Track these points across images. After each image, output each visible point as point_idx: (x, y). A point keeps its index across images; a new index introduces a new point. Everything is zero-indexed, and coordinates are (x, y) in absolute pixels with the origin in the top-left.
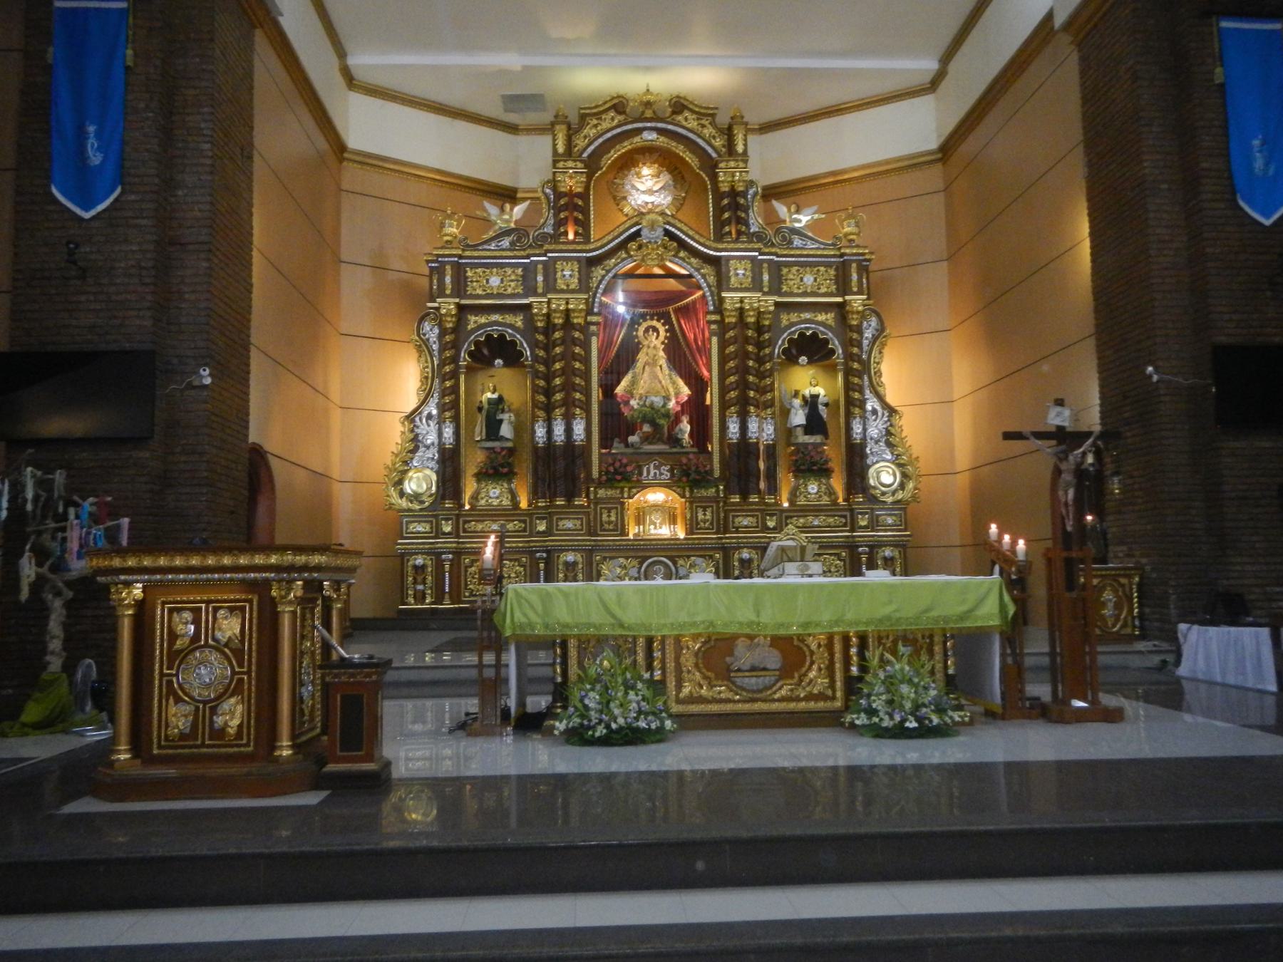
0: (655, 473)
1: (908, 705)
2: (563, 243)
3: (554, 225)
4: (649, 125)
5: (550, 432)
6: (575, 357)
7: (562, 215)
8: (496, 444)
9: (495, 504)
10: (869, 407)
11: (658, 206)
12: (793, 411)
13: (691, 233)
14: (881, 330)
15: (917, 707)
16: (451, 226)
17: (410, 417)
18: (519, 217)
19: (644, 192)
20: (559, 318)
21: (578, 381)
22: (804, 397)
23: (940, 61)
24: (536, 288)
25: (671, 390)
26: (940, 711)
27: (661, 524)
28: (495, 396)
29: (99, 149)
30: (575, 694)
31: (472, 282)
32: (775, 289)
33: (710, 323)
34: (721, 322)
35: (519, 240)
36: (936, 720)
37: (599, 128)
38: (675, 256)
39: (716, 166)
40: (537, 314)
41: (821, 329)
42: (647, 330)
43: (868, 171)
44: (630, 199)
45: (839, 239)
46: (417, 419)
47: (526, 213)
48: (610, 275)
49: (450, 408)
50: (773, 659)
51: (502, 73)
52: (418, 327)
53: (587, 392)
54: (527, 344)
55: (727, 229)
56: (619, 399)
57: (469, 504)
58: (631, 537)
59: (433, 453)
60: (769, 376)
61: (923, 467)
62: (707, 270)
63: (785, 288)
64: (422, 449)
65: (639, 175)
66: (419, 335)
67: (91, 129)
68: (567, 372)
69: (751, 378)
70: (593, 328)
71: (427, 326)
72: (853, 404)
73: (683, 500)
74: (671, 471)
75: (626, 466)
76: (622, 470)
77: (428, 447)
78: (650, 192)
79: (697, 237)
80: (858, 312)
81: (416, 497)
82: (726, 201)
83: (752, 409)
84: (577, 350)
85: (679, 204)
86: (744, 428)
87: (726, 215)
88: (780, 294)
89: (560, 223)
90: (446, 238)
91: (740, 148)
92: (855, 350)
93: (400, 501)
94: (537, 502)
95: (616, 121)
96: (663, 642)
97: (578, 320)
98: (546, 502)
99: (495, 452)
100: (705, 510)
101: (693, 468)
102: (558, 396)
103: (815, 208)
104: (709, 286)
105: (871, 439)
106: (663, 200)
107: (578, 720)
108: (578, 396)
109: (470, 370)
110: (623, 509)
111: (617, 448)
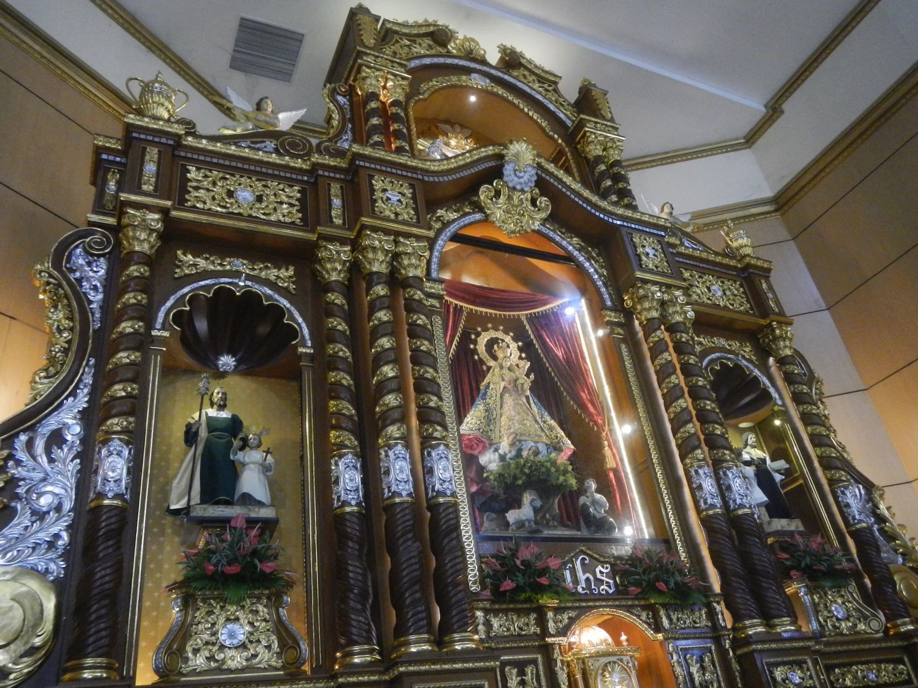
0: (588, 580)
9: (232, 664)
23: (766, 106)
28: (225, 415)
31: (197, 188)
42: (491, 343)
54: (302, 315)
59: (59, 527)
73: (660, 636)
86: (724, 490)
98: (371, 652)
110: (550, 664)
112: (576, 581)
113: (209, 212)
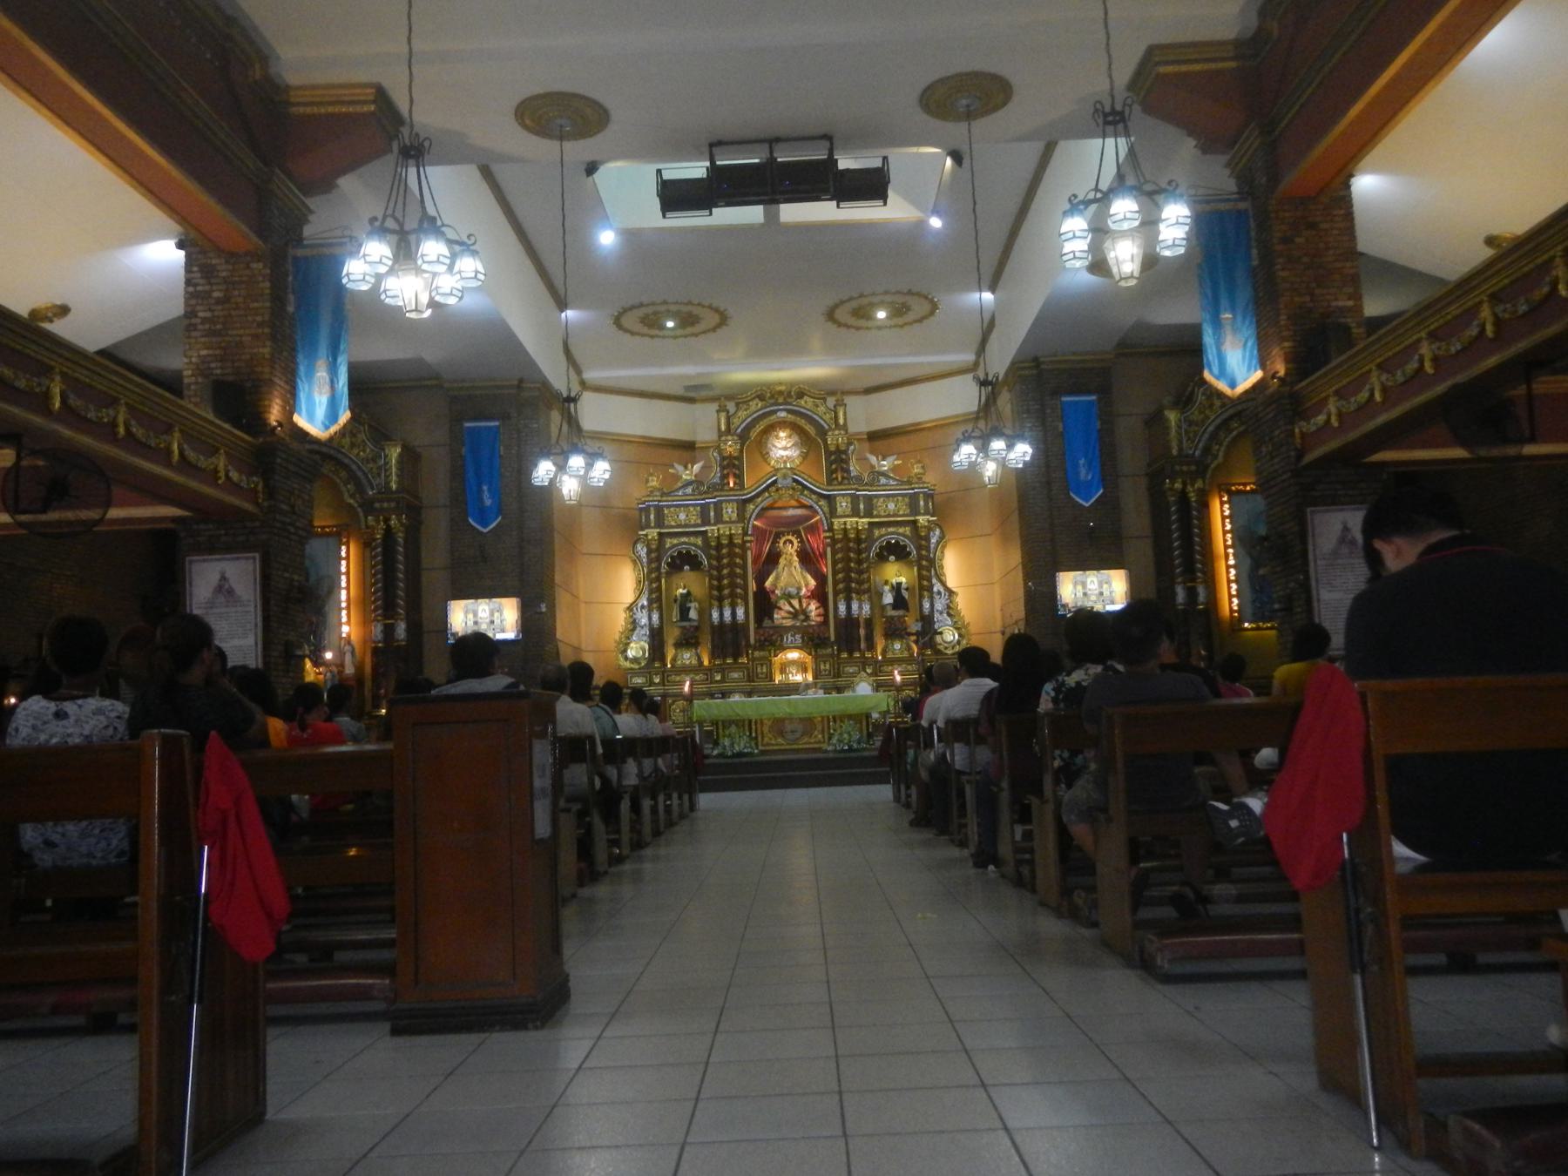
1: (846, 741)
2: (727, 490)
5: (721, 615)
6: (736, 565)
7: (725, 472)
8: (685, 624)
10: (935, 589)
11: (791, 457)
13: (810, 480)
14: (942, 537)
16: (653, 481)
17: (630, 608)
18: (698, 471)
22: (892, 585)
24: (710, 521)
25: (802, 582)
26: (859, 743)
28: (685, 591)
29: (489, 498)
30: (721, 741)
32: (868, 514)
33: (826, 538)
34: (832, 538)
35: (697, 488)
36: (855, 746)
38: (802, 494)
39: (826, 434)
42: (785, 543)
49: (657, 601)
53: (745, 588)
55: (834, 476)
57: (671, 663)
59: (646, 631)
60: (866, 572)
61: (972, 629)
63: (875, 513)
64: (638, 629)
65: (777, 437)
66: (634, 553)
67: (485, 488)
68: (732, 575)
69: (853, 575)
70: (748, 545)
71: (639, 547)
74: (802, 638)
75: (772, 635)
76: (769, 639)
77: (642, 627)
80: (925, 527)
81: (635, 660)
82: (833, 457)
83: (854, 595)
84: (738, 560)
85: (804, 456)
86: (849, 608)
87: (834, 467)
88: (871, 516)
89: (724, 477)
91: (841, 421)
93: (625, 663)
95: (760, 405)
96: (756, 722)
97: (738, 541)
101: (816, 635)
102: (726, 592)
103: (895, 457)
104: (824, 513)
105: (937, 611)
106: (794, 453)
107: (722, 751)
108: (739, 591)
109: (668, 574)
111: (767, 623)
112: (787, 640)
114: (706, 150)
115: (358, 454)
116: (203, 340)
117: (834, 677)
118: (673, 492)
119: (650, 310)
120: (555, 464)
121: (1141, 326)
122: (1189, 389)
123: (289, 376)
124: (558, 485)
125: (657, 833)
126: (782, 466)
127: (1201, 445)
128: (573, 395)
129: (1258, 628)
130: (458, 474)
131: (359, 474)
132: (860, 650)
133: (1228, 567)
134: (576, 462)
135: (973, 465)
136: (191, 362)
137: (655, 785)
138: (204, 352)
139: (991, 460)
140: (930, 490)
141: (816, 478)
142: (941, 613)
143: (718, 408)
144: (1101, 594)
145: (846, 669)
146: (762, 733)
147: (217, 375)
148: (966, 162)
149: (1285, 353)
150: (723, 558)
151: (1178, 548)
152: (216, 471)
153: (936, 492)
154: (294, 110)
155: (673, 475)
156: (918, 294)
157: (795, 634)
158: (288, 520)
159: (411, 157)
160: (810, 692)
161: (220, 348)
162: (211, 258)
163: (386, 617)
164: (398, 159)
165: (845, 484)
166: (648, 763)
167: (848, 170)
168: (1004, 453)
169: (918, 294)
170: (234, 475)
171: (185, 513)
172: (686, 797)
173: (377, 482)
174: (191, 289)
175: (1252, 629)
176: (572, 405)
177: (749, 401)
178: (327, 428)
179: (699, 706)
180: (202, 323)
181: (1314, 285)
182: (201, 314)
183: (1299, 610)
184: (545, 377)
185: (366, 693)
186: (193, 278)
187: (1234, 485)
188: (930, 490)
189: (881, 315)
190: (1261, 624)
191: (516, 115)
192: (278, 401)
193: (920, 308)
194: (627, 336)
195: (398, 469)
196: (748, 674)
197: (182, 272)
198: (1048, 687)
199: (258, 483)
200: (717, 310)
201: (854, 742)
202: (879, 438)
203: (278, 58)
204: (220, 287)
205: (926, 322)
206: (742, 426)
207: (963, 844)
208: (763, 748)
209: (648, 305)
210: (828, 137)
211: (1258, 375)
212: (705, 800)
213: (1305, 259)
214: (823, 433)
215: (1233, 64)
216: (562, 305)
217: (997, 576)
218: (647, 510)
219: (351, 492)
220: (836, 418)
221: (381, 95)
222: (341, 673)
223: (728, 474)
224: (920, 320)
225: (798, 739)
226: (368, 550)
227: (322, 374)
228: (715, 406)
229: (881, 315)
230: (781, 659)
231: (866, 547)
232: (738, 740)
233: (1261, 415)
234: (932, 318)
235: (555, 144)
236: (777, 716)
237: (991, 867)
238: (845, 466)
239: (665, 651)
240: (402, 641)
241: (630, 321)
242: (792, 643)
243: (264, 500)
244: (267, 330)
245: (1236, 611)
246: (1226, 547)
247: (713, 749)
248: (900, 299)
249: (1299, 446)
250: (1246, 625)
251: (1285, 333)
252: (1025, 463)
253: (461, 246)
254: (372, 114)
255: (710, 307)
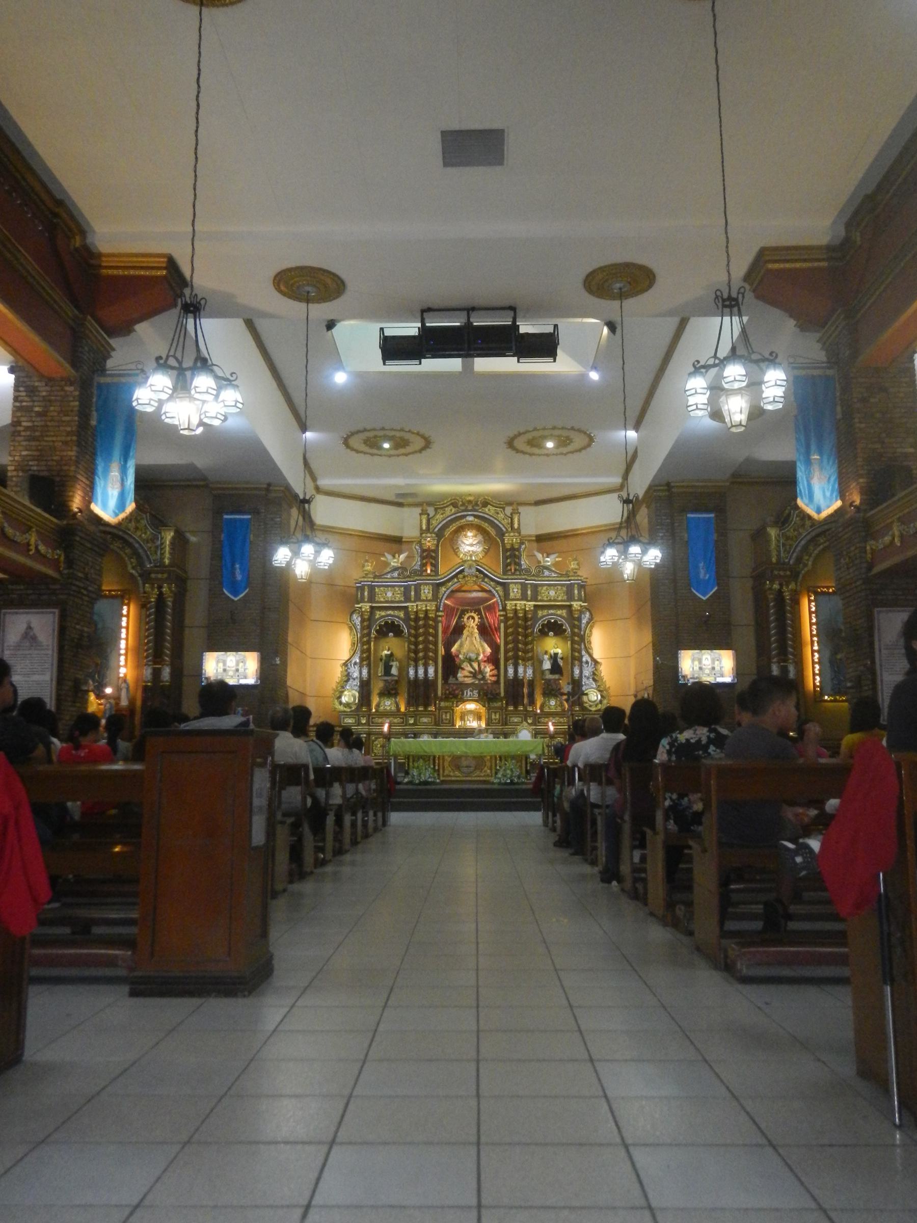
1: (509, 776)
2: (424, 576)
3: (420, 565)
4: (470, 513)
5: (416, 672)
6: (430, 634)
7: (424, 561)
10: (584, 659)
12: (544, 662)
13: (490, 570)
14: (591, 619)
15: (511, 776)
16: (368, 566)
17: (345, 664)
18: (402, 560)
19: (467, 545)
20: (422, 614)
21: (431, 646)
24: (411, 598)
25: (481, 650)
26: (519, 777)
27: (473, 720)
28: (389, 653)
30: (411, 772)
32: (534, 598)
34: (505, 616)
35: (402, 573)
36: (516, 780)
37: (444, 515)
38: (483, 581)
40: (411, 611)
41: (559, 618)
42: (468, 618)
43: (590, 530)
44: (461, 549)
45: (569, 571)
46: (349, 665)
47: (407, 557)
48: (449, 591)
49: (367, 659)
50: (473, 763)
51: (396, 486)
52: (350, 619)
53: (436, 652)
55: (509, 568)
56: (454, 654)
58: (457, 727)
59: (357, 682)
60: (531, 644)
62: (499, 588)
63: (539, 598)
64: (351, 680)
65: (466, 536)
66: (351, 621)
67: (237, 566)
68: (426, 642)
71: (355, 616)
72: (575, 657)
73: (484, 708)
75: (454, 690)
76: (453, 692)
78: (472, 545)
79: (492, 572)
80: (578, 610)
81: (347, 705)
82: (508, 554)
83: (520, 661)
84: (431, 630)
85: (486, 552)
86: (516, 671)
87: (509, 561)
88: (536, 600)
89: (423, 565)
90: (366, 572)
91: (516, 526)
92: (576, 630)
94: (409, 708)
97: (432, 615)
99: (389, 683)
100: (495, 713)
101: (489, 692)
103: (557, 555)
104: (499, 596)
105: (585, 676)
106: (478, 549)
108: (431, 654)
111: (451, 680)
112: (467, 693)
113: (381, 602)
114: (419, 315)
115: (140, 536)
116: (24, 443)
117: (501, 726)
118: (383, 575)
119: (371, 434)
120: (291, 550)
121: (749, 461)
122: (787, 512)
123: (89, 474)
124: (293, 566)
125: (354, 843)
126: (469, 559)
127: (795, 555)
128: (307, 498)
129: (835, 701)
130: (217, 555)
131: (140, 551)
132: (523, 705)
133: (813, 651)
134: (308, 549)
135: (615, 564)
136: (14, 460)
137: (357, 804)
138: (24, 453)
139: (630, 561)
140: (582, 582)
141: (495, 569)
142: (588, 678)
143: (421, 512)
144: (713, 668)
145: (512, 719)
146: (444, 767)
147: (34, 471)
148: (618, 331)
149: (861, 488)
150: (419, 629)
151: (775, 634)
152: (28, 544)
153: (589, 583)
154: (104, 272)
155: (384, 561)
156: (579, 431)
157: (473, 689)
158: (81, 585)
159: (191, 312)
160: (483, 736)
161: (38, 450)
162: (34, 382)
163: (155, 663)
164: (180, 312)
165: (517, 575)
166: (350, 788)
167: (527, 334)
168: (640, 556)
169: (579, 431)
170: (42, 548)
171: (6, 576)
172: (380, 814)
173: (154, 558)
174: (18, 404)
175: (831, 701)
176: (306, 505)
177: (447, 506)
178: (117, 515)
179: (394, 741)
180: (24, 431)
181: (884, 435)
182: (24, 424)
183: (866, 688)
184: (289, 484)
185: (136, 719)
186: (20, 396)
187: (819, 587)
188: (582, 582)
189: (550, 445)
190: (838, 697)
191: (274, 283)
192: (79, 492)
193: (579, 441)
194: (353, 452)
195: (171, 549)
196: (435, 719)
197: (12, 390)
198: (665, 742)
199: (60, 556)
200: (423, 437)
201: (515, 776)
202: (544, 540)
203: (94, 232)
204: (39, 404)
205: (584, 452)
206: (439, 526)
207: (593, 863)
208: (444, 779)
209: (369, 431)
210: (513, 309)
211: (839, 503)
212: (396, 818)
213: (878, 415)
214: (501, 534)
215: (824, 264)
216: (304, 429)
217: (632, 652)
218: (362, 589)
219: (134, 564)
220: (512, 523)
221: (171, 264)
222: (117, 704)
223: (427, 563)
224: (580, 450)
225: (471, 772)
226: (144, 611)
227: (115, 473)
228: (419, 510)
229: (550, 445)
230: (462, 709)
231: (531, 624)
232: (424, 771)
233: (840, 535)
234: (588, 449)
235: (304, 305)
236: (455, 754)
237: (614, 883)
238: (517, 560)
239: (372, 698)
240: (167, 681)
241: (355, 442)
242: (470, 697)
243: (64, 569)
244: (75, 438)
245: (818, 686)
246: (812, 636)
247: (404, 777)
248: (565, 433)
249: (870, 561)
250: (826, 697)
251: (861, 472)
252: (656, 564)
253: (225, 381)
254: (165, 277)
255: (418, 434)
